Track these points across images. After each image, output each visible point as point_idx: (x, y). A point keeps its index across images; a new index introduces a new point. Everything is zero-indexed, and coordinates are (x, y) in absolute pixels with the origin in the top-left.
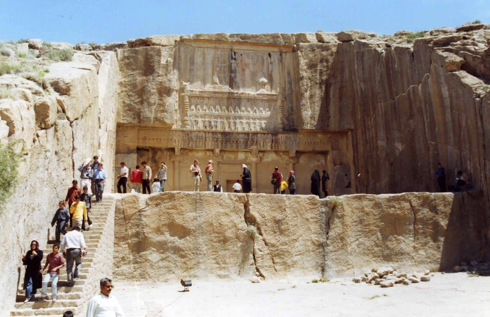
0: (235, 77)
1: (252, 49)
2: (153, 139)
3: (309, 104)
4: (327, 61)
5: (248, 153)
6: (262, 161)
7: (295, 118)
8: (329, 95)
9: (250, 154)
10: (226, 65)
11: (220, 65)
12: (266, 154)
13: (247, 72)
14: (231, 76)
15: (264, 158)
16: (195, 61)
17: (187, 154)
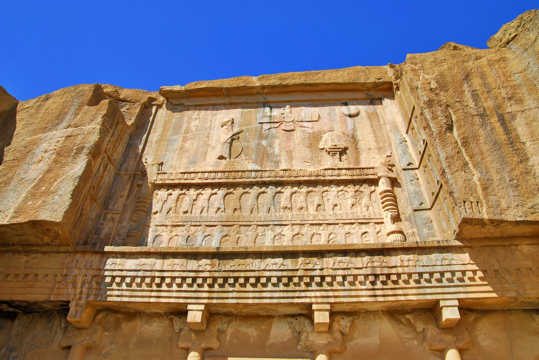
0: (271, 145)
1: (307, 98)
2: (17, 275)
3: (467, 159)
4: (483, 76)
5: (302, 319)
6: (350, 345)
7: (432, 218)
8: (517, 136)
9: (307, 322)
10: (250, 127)
11: (236, 130)
12: (360, 323)
13: (298, 135)
14: (259, 144)
15: (356, 335)
16: (185, 126)
17: (117, 326)
